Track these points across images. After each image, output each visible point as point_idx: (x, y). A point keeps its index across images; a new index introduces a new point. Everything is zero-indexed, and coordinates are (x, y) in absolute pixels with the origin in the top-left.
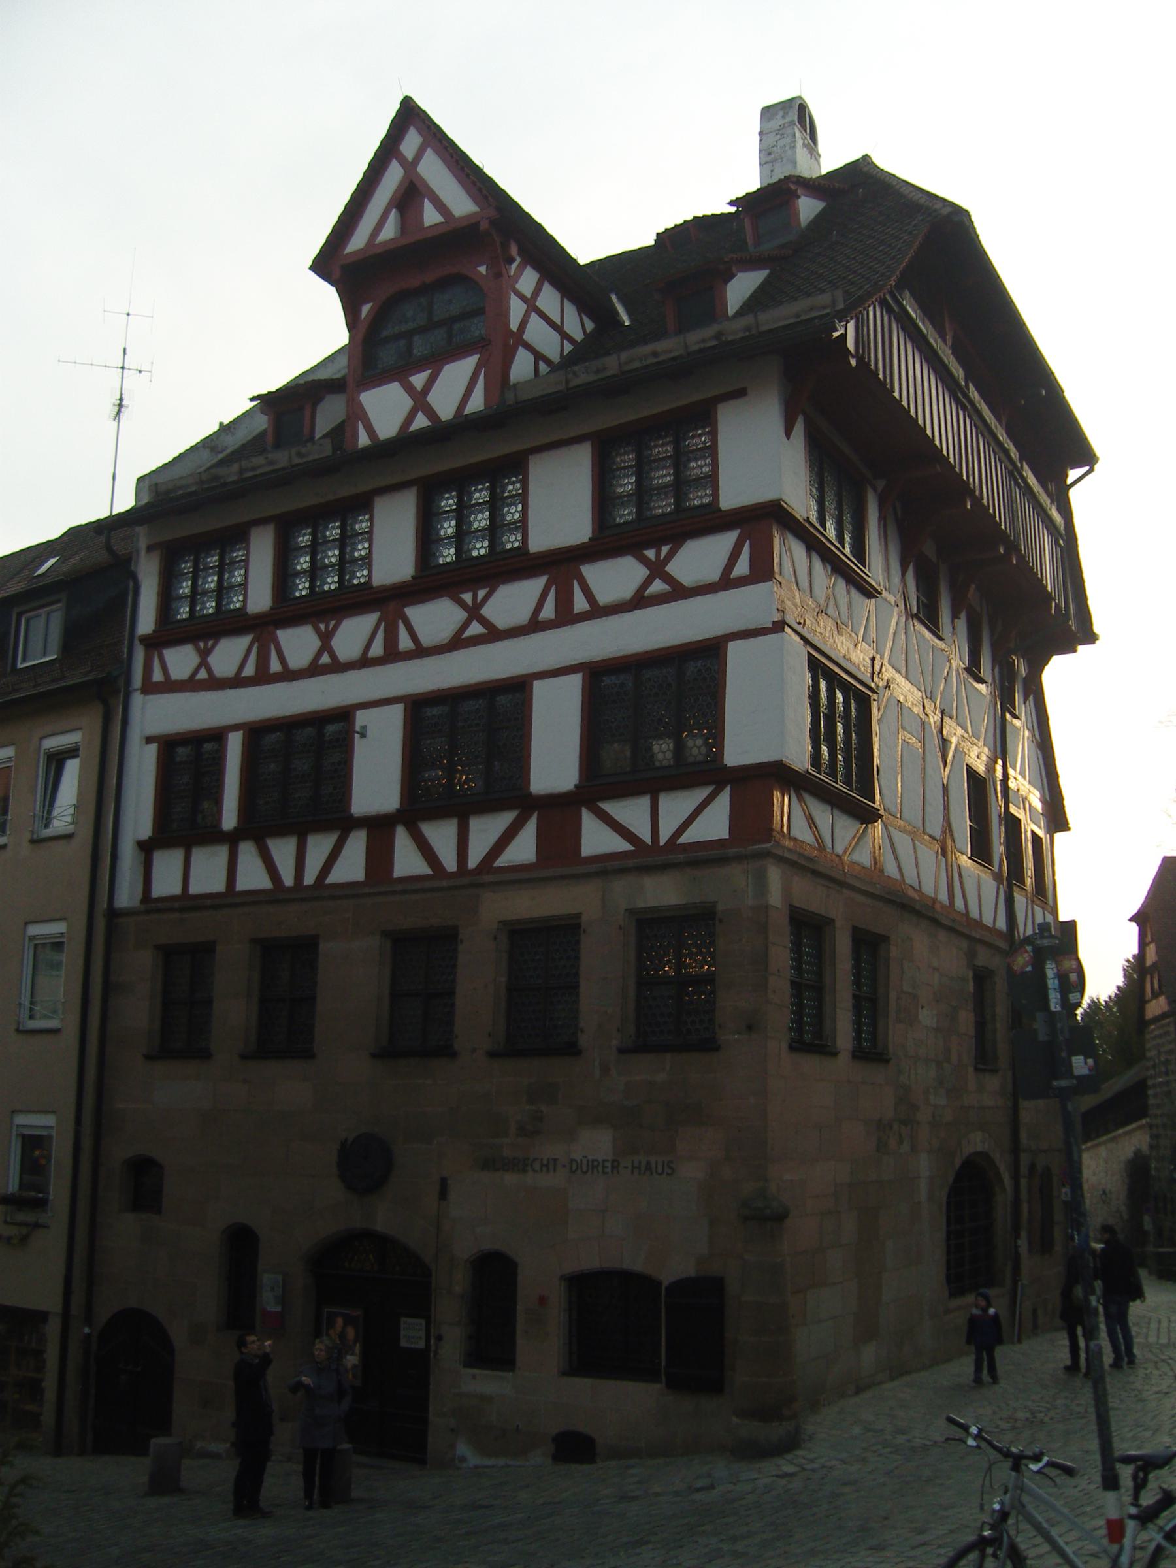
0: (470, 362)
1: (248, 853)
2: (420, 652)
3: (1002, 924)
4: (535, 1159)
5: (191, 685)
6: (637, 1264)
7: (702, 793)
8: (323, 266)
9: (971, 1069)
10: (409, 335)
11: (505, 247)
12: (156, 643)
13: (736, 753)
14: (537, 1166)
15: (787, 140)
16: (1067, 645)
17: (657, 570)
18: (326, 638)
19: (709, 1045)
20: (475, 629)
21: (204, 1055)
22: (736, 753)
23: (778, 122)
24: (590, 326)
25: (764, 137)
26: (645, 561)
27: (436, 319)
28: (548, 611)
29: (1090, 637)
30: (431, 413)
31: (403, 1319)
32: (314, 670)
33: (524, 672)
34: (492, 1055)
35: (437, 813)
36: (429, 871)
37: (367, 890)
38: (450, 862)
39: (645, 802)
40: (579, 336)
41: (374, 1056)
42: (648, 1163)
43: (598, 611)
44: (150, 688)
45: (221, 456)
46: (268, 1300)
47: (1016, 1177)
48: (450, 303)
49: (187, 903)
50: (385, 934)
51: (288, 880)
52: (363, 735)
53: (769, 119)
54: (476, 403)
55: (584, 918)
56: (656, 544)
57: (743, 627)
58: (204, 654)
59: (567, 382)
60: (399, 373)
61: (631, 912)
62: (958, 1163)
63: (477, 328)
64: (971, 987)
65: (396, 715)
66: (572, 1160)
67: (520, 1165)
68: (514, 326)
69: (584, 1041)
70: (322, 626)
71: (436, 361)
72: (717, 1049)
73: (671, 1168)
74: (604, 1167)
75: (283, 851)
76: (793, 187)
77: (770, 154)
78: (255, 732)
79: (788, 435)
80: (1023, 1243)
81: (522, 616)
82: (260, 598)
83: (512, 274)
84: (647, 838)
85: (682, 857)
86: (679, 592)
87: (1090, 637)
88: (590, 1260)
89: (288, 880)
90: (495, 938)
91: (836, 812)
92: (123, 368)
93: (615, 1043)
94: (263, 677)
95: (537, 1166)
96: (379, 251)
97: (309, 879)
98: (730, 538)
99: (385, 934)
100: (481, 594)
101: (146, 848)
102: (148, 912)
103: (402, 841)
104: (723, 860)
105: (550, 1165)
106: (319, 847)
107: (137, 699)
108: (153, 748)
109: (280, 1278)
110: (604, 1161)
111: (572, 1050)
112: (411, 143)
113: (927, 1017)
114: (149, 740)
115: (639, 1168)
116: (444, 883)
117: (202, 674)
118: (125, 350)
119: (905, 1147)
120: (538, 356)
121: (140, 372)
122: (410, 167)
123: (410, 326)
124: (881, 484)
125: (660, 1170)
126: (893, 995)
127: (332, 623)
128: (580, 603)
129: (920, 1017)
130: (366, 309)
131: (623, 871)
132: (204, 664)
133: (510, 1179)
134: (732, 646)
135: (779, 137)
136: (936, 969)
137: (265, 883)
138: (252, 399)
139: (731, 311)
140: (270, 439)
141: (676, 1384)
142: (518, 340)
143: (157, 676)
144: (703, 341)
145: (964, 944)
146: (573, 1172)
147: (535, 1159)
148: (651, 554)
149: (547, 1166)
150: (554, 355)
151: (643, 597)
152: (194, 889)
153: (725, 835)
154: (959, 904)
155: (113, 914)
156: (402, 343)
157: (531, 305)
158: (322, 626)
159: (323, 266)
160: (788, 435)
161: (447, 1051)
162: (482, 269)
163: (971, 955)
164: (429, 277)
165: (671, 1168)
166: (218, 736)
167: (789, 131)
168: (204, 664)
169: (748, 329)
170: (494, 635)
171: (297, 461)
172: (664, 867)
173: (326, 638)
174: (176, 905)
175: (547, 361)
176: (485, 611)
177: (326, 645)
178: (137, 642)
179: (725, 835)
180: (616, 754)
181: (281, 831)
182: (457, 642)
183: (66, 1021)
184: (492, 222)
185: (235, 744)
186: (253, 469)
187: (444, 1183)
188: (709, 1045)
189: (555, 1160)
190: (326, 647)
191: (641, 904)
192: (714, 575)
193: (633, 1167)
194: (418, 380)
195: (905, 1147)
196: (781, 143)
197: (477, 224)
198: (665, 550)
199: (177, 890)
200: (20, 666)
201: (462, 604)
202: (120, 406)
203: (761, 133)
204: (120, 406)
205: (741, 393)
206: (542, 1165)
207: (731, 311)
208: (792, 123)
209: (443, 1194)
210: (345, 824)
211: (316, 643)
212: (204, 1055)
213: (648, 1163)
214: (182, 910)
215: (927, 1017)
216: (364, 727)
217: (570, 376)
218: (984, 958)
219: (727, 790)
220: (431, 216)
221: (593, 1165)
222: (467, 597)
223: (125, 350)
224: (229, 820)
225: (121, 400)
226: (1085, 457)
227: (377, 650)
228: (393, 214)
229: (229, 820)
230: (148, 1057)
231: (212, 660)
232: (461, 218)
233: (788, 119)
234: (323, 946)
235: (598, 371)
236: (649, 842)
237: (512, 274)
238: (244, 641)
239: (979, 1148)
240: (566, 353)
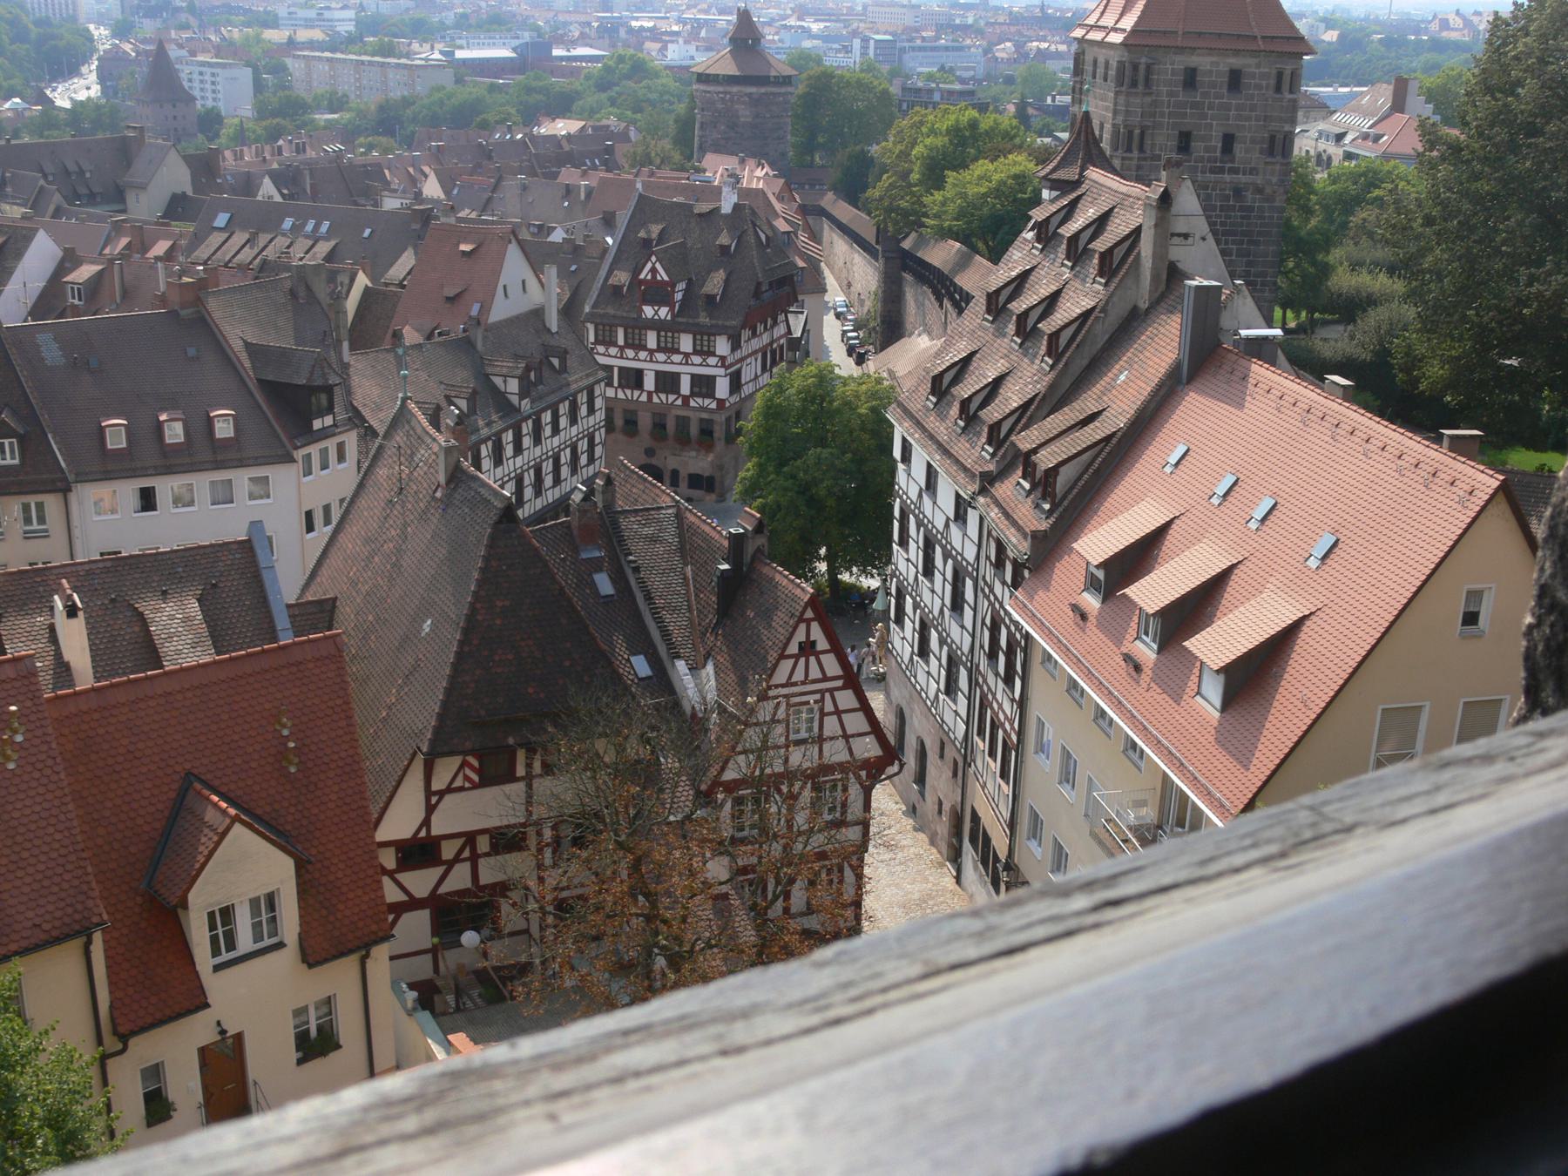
1: (619, 390)
13: (717, 396)
22: (717, 396)
32: (634, 359)
54: (669, 318)
65: (653, 373)
75: (628, 392)
78: (621, 369)
82: (621, 342)
86: (708, 365)
94: (622, 357)
103: (654, 395)
106: (636, 393)
170: (672, 363)
180: (696, 390)
182: (665, 362)
185: (616, 370)
224: (616, 384)
229: (616, 384)
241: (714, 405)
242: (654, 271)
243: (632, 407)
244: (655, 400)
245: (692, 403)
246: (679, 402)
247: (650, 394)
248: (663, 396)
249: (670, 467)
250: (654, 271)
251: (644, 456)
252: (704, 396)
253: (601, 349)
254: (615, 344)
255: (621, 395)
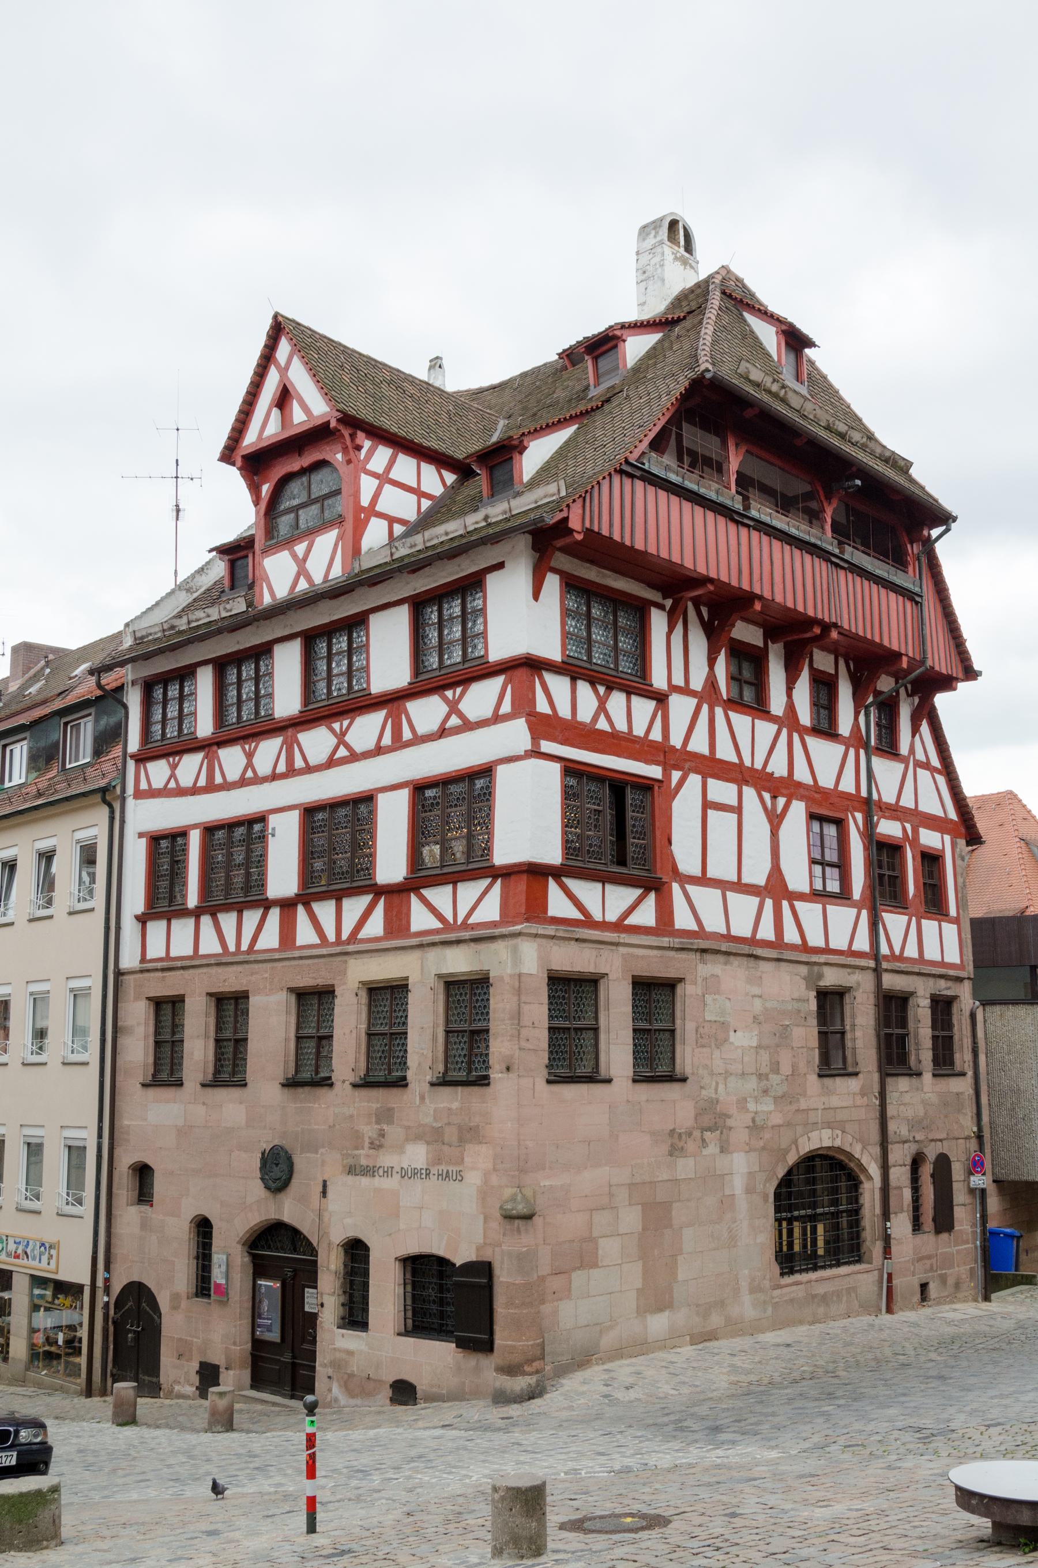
0: (332, 535)
2: (309, 769)
3: (862, 943)
4: (380, 1167)
5: (163, 793)
6: (441, 1252)
7: (485, 883)
8: (227, 456)
9: (813, 1078)
10: (296, 509)
11: (353, 436)
12: (141, 759)
13: (502, 855)
14: (381, 1172)
15: (657, 259)
16: (947, 683)
17: (453, 708)
18: (250, 756)
19: (483, 1081)
20: (343, 752)
21: (179, 1084)
22: (502, 855)
23: (651, 241)
24: (450, 478)
25: (640, 257)
26: (445, 699)
27: (313, 497)
28: (387, 740)
29: (970, 674)
30: (309, 579)
31: (306, 1290)
32: (243, 782)
33: (372, 787)
34: (355, 1086)
35: (322, 896)
36: (319, 942)
37: (277, 956)
38: (331, 936)
39: (449, 888)
40: (437, 490)
41: (283, 1085)
42: (448, 1172)
43: (419, 740)
44: (139, 794)
45: (195, 595)
46: (218, 1276)
47: (885, 1168)
48: (321, 484)
49: (169, 965)
50: (291, 990)
51: (232, 948)
52: (273, 835)
53: (644, 240)
55: (410, 981)
56: (452, 685)
57: (506, 755)
58: (174, 767)
59: (392, 555)
60: (288, 543)
61: (439, 976)
62: (792, 1159)
63: (341, 505)
64: (813, 1005)
65: (293, 818)
66: (402, 1168)
67: (369, 1171)
68: (365, 502)
69: (410, 1075)
70: (247, 747)
71: (313, 532)
72: (488, 1084)
73: (461, 1175)
74: (421, 1174)
75: (228, 921)
76: (618, 333)
77: (644, 272)
78: (209, 830)
79: (536, 596)
80: (900, 1225)
81: (371, 745)
82: (204, 727)
83: (362, 458)
84: (449, 917)
85: (466, 935)
86: (468, 726)
87: (970, 674)
88: (413, 1248)
89: (232, 948)
90: (357, 995)
91: (608, 887)
92: (177, 477)
93: (428, 1078)
94: (211, 788)
95: (381, 1172)
96: (265, 444)
97: (244, 947)
98: (499, 681)
99: (291, 990)
100: (346, 723)
101: (142, 920)
102: (142, 971)
104: (492, 938)
105: (388, 1172)
106: (251, 918)
107: (130, 802)
108: (143, 841)
109: (225, 1257)
110: (421, 1169)
111: (401, 1083)
112: (284, 349)
113: (743, 1039)
114: (141, 835)
115: (442, 1175)
116: (324, 951)
117: (172, 785)
118: (177, 460)
119: (713, 1149)
120: (391, 520)
121: (192, 479)
122: (284, 371)
123: (296, 502)
124: (668, 603)
125: (454, 1178)
126: (690, 1026)
127: (253, 745)
128: (407, 735)
129: (732, 1039)
130: (266, 489)
131: (433, 944)
132: (173, 775)
133: (365, 1181)
134: (501, 770)
135: (651, 255)
136: (760, 997)
137: (218, 950)
138: (210, 551)
139: (526, 478)
140: (227, 582)
141: (463, 1344)
142: (372, 511)
143: (144, 785)
144: (477, 523)
145: (804, 970)
146: (403, 1177)
147: (380, 1167)
148: (449, 694)
149: (387, 1172)
150: (411, 516)
151: (445, 729)
152: (173, 954)
153: (497, 918)
154: (791, 936)
155: (119, 973)
156: (292, 515)
157: (384, 478)
158: (247, 747)
159: (227, 456)
160: (536, 596)
161: (327, 1083)
162: (339, 456)
163: (811, 980)
164: (306, 460)
165: (461, 1175)
166: (182, 834)
167: (659, 250)
168: (173, 775)
169: (505, 512)
171: (224, 614)
172: (458, 942)
173: (250, 756)
174: (159, 965)
175: (402, 522)
176: (347, 738)
177: (250, 765)
178: (128, 758)
179: (497, 918)
180: (432, 852)
181: (227, 908)
182: (331, 763)
183: (92, 1055)
184: (339, 420)
186: (197, 620)
187: (325, 1182)
188: (483, 1081)
189: (392, 1168)
190: (250, 765)
191: (444, 971)
192: (488, 713)
193: (438, 1175)
194: (300, 549)
195: (713, 1149)
196: (653, 262)
197: (328, 422)
198: (459, 690)
199: (163, 954)
200: (68, 766)
201: (333, 731)
202: (178, 511)
203: (638, 253)
204: (178, 511)
205: (500, 566)
206: (384, 1172)
207: (526, 478)
208: (661, 243)
209: (324, 1193)
210: (267, 905)
211: (244, 761)
212: (179, 1084)
213: (448, 1172)
214: (163, 970)
215: (743, 1039)
216: (274, 829)
217: (394, 550)
218: (831, 978)
219: (499, 881)
220: (298, 416)
221: (415, 1173)
222: (336, 726)
223: (177, 460)
225: (177, 506)
226: (944, 518)
227: (282, 768)
228: (275, 412)
229: (192, 900)
230: (144, 1085)
231: (177, 772)
232: (318, 417)
233: (659, 239)
234: (253, 1000)
235: (411, 547)
236: (452, 922)
237: (362, 458)
238: (199, 756)
239: (827, 1143)
240: (422, 510)
241: (490, 910)
242: (284, 398)
243: (229, 981)
244: (305, 934)
245: (420, 919)
246: (375, 926)
247: (288, 905)
248: (325, 911)
249: (338, 1235)
250: (284, 398)
251: (257, 1189)
252: (453, 878)
253: (158, 772)
254: (194, 746)
255: (210, 945)
